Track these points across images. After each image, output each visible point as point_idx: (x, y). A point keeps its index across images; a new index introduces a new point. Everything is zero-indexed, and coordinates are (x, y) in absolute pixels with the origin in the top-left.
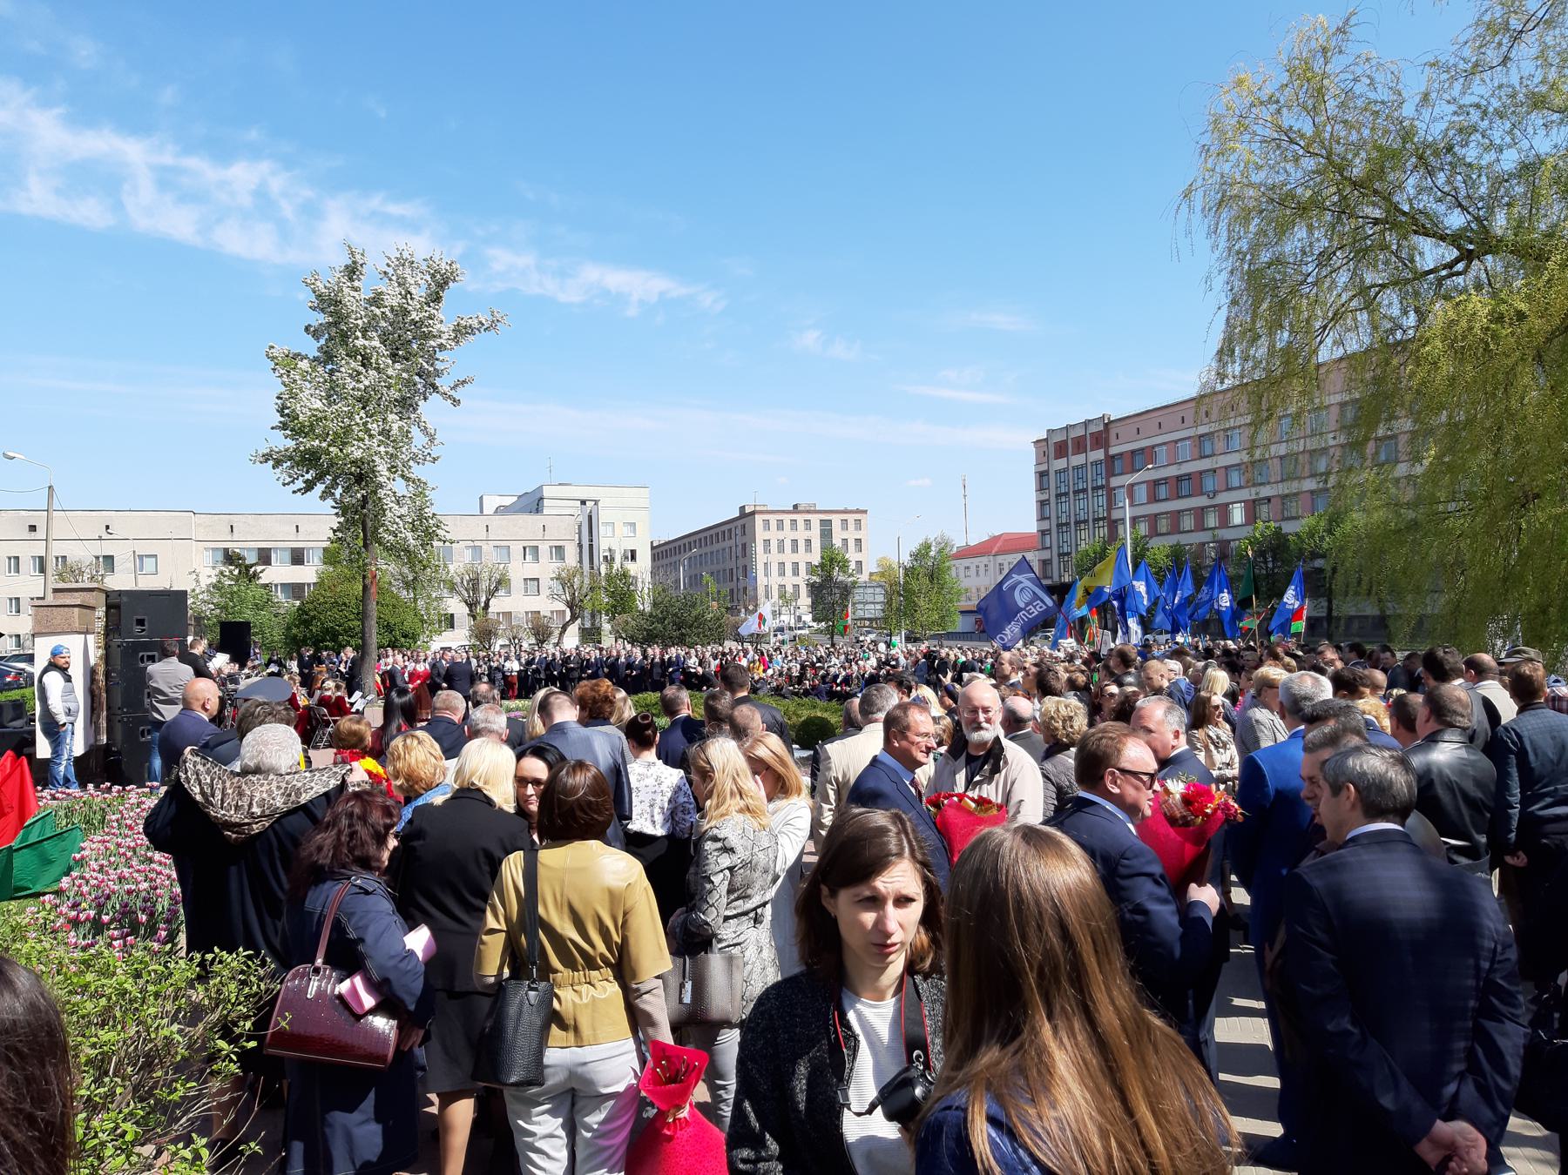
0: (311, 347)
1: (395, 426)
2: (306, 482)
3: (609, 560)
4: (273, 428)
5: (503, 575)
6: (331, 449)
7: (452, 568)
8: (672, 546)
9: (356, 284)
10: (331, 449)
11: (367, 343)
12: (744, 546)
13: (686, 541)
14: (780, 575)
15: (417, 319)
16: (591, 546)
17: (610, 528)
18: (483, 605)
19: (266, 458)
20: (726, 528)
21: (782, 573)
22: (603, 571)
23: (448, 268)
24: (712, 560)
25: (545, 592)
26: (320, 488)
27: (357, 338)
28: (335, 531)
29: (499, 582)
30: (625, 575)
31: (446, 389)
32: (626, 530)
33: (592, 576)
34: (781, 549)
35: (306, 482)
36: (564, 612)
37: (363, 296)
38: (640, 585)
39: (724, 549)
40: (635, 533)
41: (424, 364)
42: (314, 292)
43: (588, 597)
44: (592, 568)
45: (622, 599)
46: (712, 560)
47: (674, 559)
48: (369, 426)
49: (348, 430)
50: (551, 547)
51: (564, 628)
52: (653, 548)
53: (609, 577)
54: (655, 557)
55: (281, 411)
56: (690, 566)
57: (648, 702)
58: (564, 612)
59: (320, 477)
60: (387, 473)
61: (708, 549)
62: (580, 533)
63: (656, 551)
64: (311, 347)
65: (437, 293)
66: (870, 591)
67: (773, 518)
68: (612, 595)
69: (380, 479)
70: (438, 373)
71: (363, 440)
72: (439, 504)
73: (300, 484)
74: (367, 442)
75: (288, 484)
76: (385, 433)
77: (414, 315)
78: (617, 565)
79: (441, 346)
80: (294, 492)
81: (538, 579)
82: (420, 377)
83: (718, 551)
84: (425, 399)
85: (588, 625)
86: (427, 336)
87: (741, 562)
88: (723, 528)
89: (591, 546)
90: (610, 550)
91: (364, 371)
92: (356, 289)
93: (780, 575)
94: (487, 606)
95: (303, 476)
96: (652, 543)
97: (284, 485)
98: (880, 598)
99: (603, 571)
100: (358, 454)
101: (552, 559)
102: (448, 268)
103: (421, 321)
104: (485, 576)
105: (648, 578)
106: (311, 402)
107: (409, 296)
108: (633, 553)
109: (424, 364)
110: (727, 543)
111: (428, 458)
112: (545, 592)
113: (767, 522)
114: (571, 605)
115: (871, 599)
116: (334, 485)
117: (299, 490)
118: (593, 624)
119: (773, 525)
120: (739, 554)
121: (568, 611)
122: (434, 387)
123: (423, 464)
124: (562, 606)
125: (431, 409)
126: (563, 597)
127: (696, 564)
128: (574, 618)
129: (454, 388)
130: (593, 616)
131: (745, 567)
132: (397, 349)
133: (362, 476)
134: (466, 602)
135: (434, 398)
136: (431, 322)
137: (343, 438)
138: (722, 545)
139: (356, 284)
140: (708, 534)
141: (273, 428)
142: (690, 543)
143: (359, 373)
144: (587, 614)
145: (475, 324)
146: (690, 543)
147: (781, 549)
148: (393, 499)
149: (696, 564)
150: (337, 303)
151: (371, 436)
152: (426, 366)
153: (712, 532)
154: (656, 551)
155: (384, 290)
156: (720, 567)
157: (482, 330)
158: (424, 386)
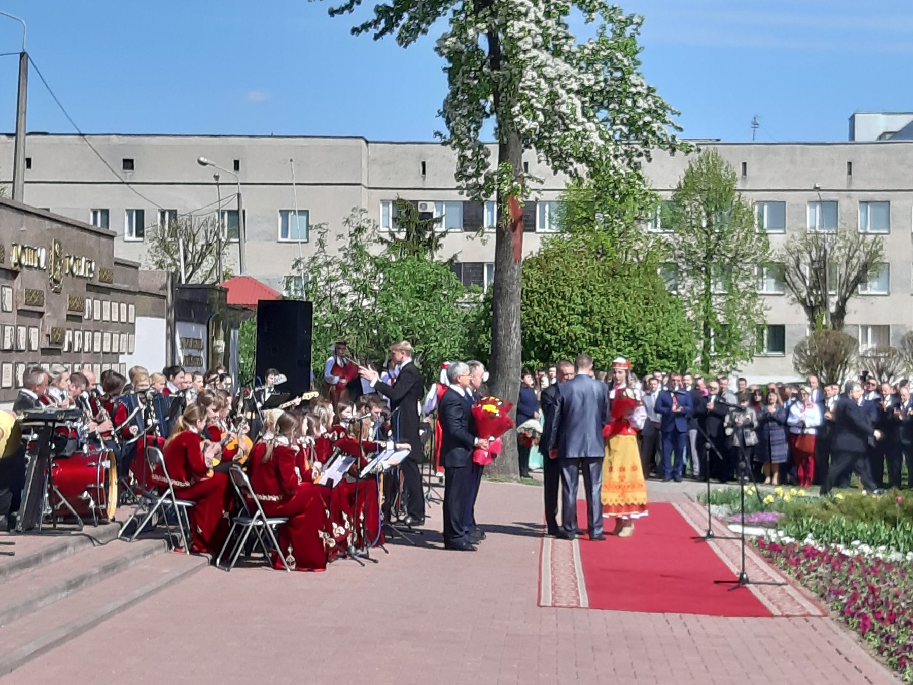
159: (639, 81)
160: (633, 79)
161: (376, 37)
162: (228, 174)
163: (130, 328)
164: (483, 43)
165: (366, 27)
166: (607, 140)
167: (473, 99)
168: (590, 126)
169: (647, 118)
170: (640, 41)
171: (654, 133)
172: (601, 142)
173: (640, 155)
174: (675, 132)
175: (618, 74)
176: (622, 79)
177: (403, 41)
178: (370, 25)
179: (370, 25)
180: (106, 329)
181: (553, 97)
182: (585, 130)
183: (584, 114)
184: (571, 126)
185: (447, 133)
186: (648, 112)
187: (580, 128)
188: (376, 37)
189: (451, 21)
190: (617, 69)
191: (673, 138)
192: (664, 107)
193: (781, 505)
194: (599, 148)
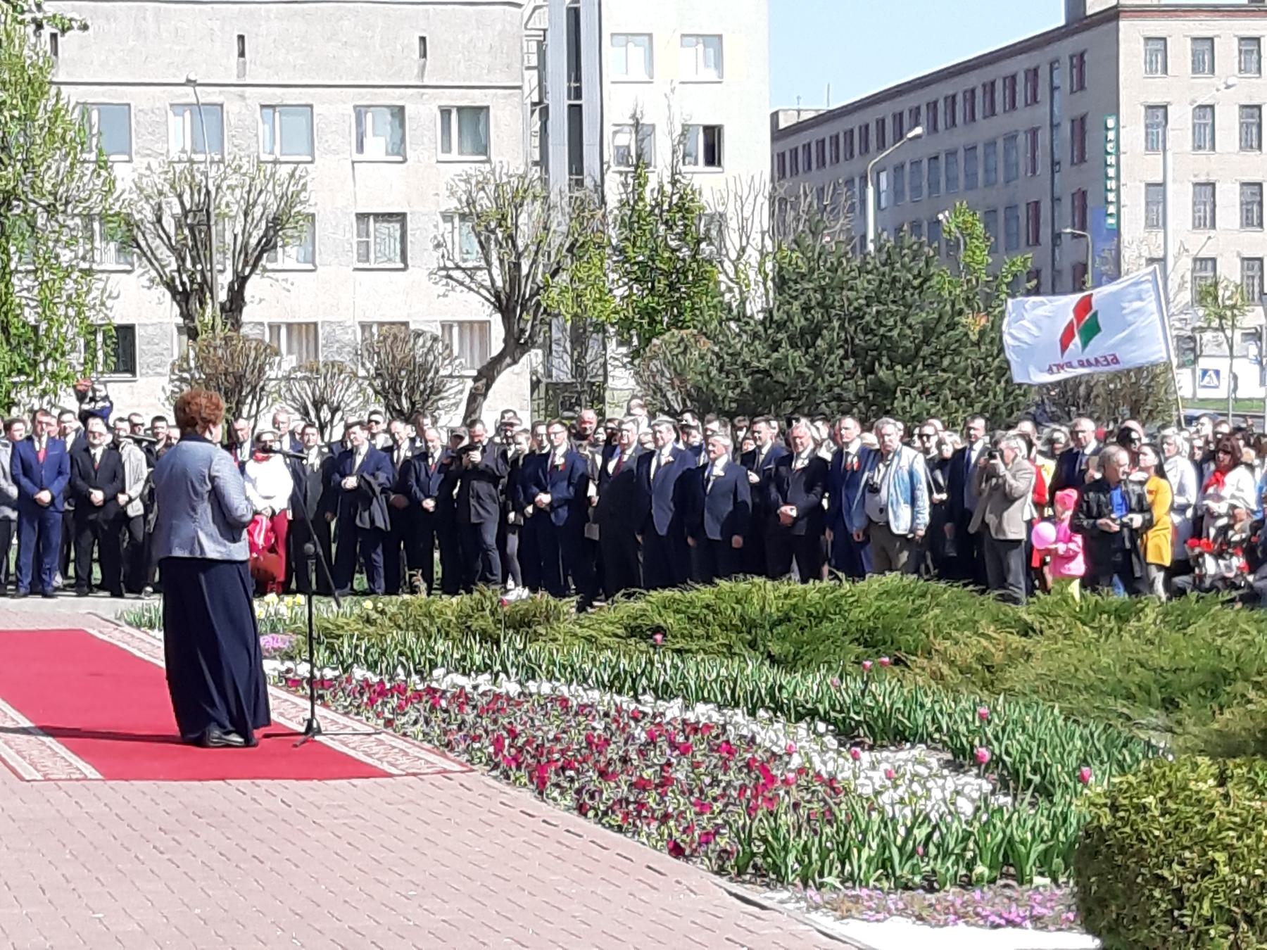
3: (638, 164)
5: (289, 201)
7: (124, 174)
8: (839, 127)
12: (1080, 125)
13: (886, 110)
14: (1199, 224)
16: (575, 113)
17: (637, 53)
18: (223, 296)
20: (1019, 65)
21: (1206, 219)
22: (614, 192)
24: (971, 176)
25: (424, 258)
29: (276, 224)
30: (684, 208)
32: (690, 61)
33: (579, 207)
34: (1204, 135)
36: (484, 326)
38: (733, 241)
39: (1011, 138)
40: (719, 64)
43: (563, 277)
44: (580, 183)
45: (672, 287)
46: (971, 176)
47: (846, 169)
50: (445, 112)
51: (488, 374)
52: (778, 135)
53: (633, 220)
54: (784, 165)
56: (897, 193)
57: (753, 611)
58: (484, 326)
61: (959, 138)
62: (541, 67)
63: (788, 144)
67: (1179, 33)
68: (643, 274)
78: (659, 174)
81: (401, 217)
83: (992, 144)
85: (563, 372)
87: (1068, 181)
88: (1009, 67)
89: (575, 113)
90: (637, 126)
93: (1199, 224)
94: (236, 301)
96: (775, 116)
99: (613, 199)
101: (447, 148)
104: (229, 201)
105: (761, 219)
108: (713, 137)
110: (1023, 118)
112: (424, 258)
113: (1158, 46)
114: (506, 304)
118: (579, 368)
119: (1180, 52)
120: (1064, 154)
121: (497, 319)
124: (478, 308)
126: (482, 276)
127: (916, 189)
128: (516, 346)
130: (579, 339)
131: (1081, 198)
134: (170, 286)
138: (1003, 123)
140: (957, 86)
142: (899, 117)
144: (560, 332)
146: (899, 117)
147: (1204, 135)
149: (916, 189)
153: (974, 80)
154: (788, 144)
156: (998, 197)
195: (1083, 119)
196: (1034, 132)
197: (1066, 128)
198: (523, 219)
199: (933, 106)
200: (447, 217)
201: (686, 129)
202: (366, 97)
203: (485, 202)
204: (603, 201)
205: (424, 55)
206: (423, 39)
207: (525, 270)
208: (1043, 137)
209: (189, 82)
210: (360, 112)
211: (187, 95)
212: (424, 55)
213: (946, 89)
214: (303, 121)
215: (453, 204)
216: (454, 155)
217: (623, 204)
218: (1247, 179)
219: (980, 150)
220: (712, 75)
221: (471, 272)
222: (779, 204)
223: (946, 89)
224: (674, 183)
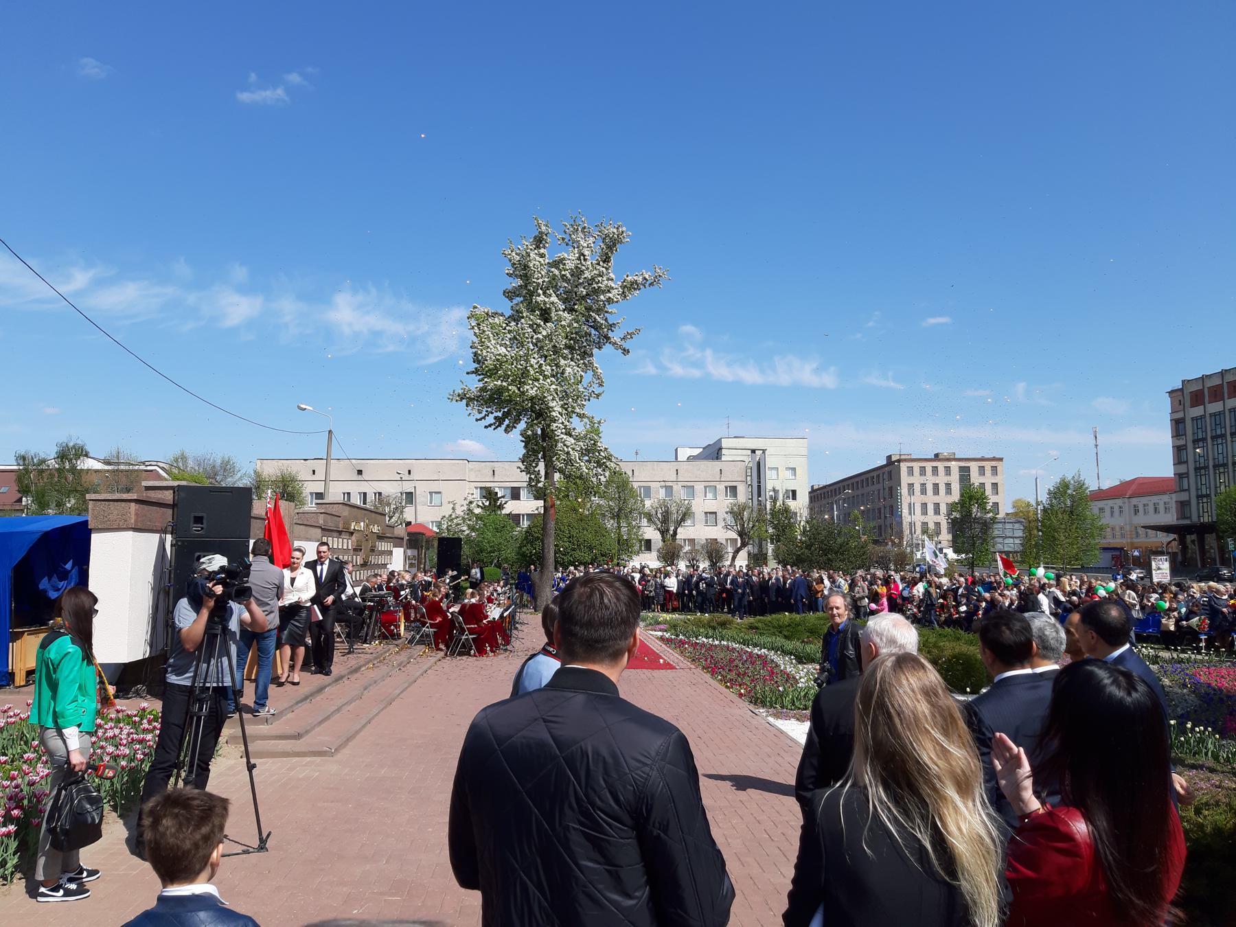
0: (506, 307)
1: (568, 370)
2: (496, 418)
3: (775, 500)
4: (468, 373)
6: (510, 388)
7: (648, 503)
8: (829, 489)
9: (542, 251)
10: (510, 388)
11: (547, 300)
12: (891, 489)
15: (590, 277)
16: (759, 487)
17: (774, 472)
18: (671, 532)
19: (462, 397)
20: (875, 474)
21: (925, 512)
22: (768, 507)
23: (615, 231)
26: (507, 422)
27: (539, 295)
28: (523, 462)
30: (786, 510)
31: (618, 340)
32: (789, 474)
34: (924, 491)
35: (496, 418)
37: (547, 261)
40: (795, 475)
41: (597, 317)
42: (510, 261)
48: (543, 368)
49: (525, 373)
50: (726, 488)
53: (774, 513)
55: (476, 360)
59: (506, 415)
60: (560, 410)
61: (859, 492)
64: (506, 307)
65: (607, 254)
66: (1010, 526)
67: (916, 466)
69: (554, 414)
70: (611, 327)
71: (538, 380)
72: (608, 441)
73: (490, 419)
74: (541, 381)
75: (481, 419)
76: (559, 376)
77: (587, 274)
79: (609, 300)
80: (486, 427)
81: (715, 513)
82: (596, 329)
84: (600, 348)
86: (597, 292)
88: (872, 474)
89: (759, 487)
90: (774, 490)
91: (542, 323)
92: (542, 256)
94: (675, 533)
95: (492, 413)
96: (812, 487)
97: (477, 420)
98: (1020, 533)
99: (768, 507)
100: (532, 392)
101: (726, 496)
102: (615, 231)
103: (593, 279)
104: (673, 509)
106: (497, 349)
107: (582, 257)
108: (794, 492)
109: (597, 317)
110: (876, 487)
111: (593, 395)
112: (721, 524)
113: (910, 470)
114: (741, 534)
115: (1010, 535)
116: (517, 421)
117: (490, 425)
119: (917, 471)
122: (607, 338)
123: (589, 400)
124: (734, 535)
125: (602, 357)
126: (735, 527)
128: (744, 545)
129: (624, 339)
131: (892, 507)
132: (575, 304)
133: (539, 412)
134: (659, 530)
135: (608, 348)
136: (600, 279)
137: (522, 377)
138: (871, 488)
139: (542, 251)
141: (468, 373)
143: (539, 326)
145: (640, 279)
147: (924, 491)
148: (564, 431)
150: (526, 267)
151: (545, 377)
152: (599, 319)
153: (864, 477)
155: (566, 255)
157: (647, 285)
158: (598, 337)
159: (602, 444)
160: (599, 444)
161: (494, 429)
162: (406, 477)
163: (390, 553)
164: (539, 432)
165: (490, 425)
166: (588, 469)
167: (535, 452)
168: (582, 464)
169: (605, 460)
170: (601, 429)
171: (607, 467)
172: (587, 471)
173: (601, 475)
174: (615, 466)
175: (593, 442)
176: (594, 444)
177: (506, 431)
178: (492, 425)
179: (492, 425)
180: (383, 554)
181: (568, 453)
182: (580, 466)
183: (580, 459)
184: (575, 464)
185: (523, 467)
186: (605, 458)
187: (578, 465)
188: (494, 429)
189: (526, 422)
190: (592, 440)
191: (615, 468)
192: (611, 455)
193: (665, 622)
194: (587, 474)
195: (892, 487)
196: (879, 490)
197: (887, 489)
198: (745, 513)
199: (853, 484)
200: (727, 513)
201: (787, 490)
202: (707, 484)
203: (735, 509)
204: (766, 509)
205: (721, 473)
206: (721, 470)
207: (746, 526)
208: (881, 491)
209: (665, 481)
210: (705, 487)
211: (663, 484)
212: (721, 473)
213: (856, 480)
214: (692, 489)
215: (728, 510)
216: (728, 498)
217: (771, 509)
218: (935, 502)
219: (865, 495)
220: (794, 477)
221: (732, 527)
222: (811, 509)
223: (856, 480)
224: (783, 504)
